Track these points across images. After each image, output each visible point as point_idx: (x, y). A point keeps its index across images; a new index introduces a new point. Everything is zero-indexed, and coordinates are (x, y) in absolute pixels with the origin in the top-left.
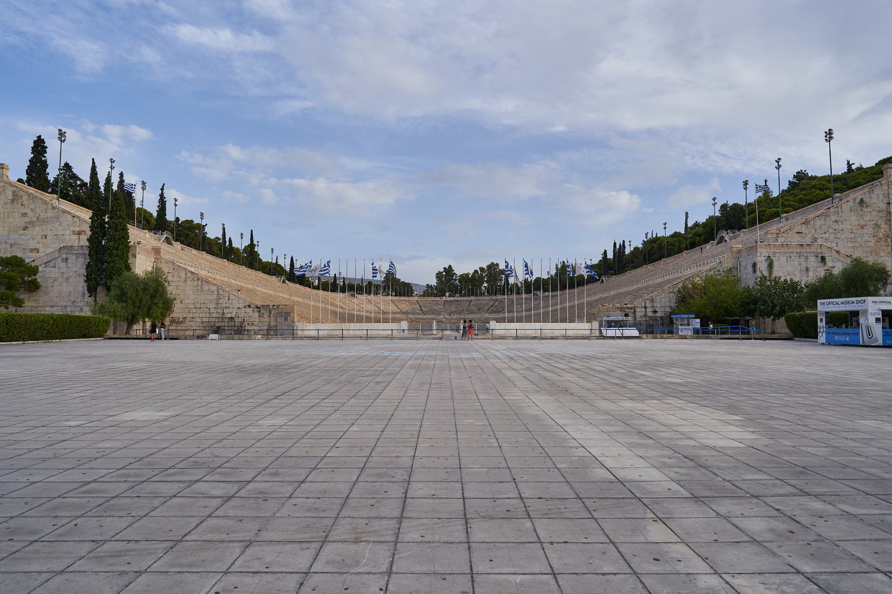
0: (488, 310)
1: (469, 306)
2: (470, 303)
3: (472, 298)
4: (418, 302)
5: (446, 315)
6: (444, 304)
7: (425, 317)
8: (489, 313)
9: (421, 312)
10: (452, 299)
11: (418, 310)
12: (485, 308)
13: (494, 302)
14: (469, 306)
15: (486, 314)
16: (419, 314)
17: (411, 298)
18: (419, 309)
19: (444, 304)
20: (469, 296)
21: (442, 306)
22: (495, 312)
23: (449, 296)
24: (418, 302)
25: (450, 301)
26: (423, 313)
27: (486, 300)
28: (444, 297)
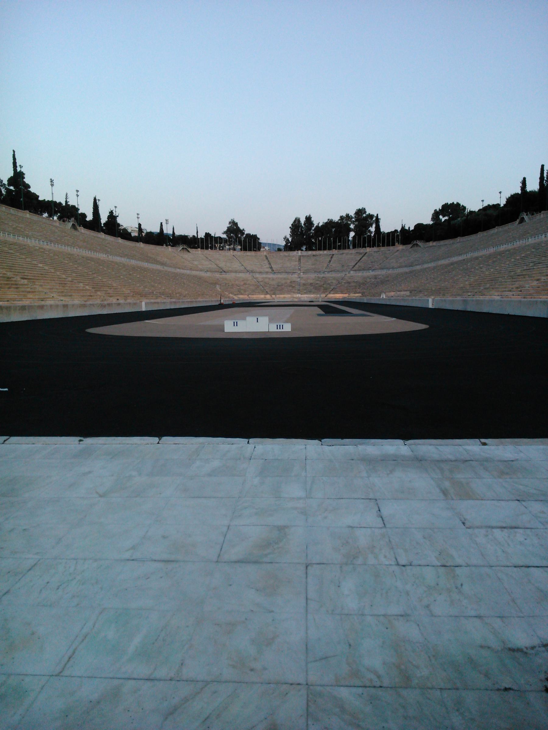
0: (354, 266)
1: (330, 261)
2: (332, 258)
3: (334, 252)
4: (267, 258)
5: (302, 274)
6: (300, 259)
7: (275, 276)
8: (354, 271)
9: (270, 270)
10: (310, 253)
11: (267, 268)
12: (350, 264)
13: (361, 256)
14: (330, 261)
15: (352, 272)
16: (267, 273)
17: (258, 253)
18: (268, 266)
19: (300, 259)
20: (330, 249)
21: (297, 263)
22: (364, 270)
23: (306, 250)
24: (267, 258)
25: (308, 256)
26: (273, 271)
27: (351, 254)
28: (300, 252)
